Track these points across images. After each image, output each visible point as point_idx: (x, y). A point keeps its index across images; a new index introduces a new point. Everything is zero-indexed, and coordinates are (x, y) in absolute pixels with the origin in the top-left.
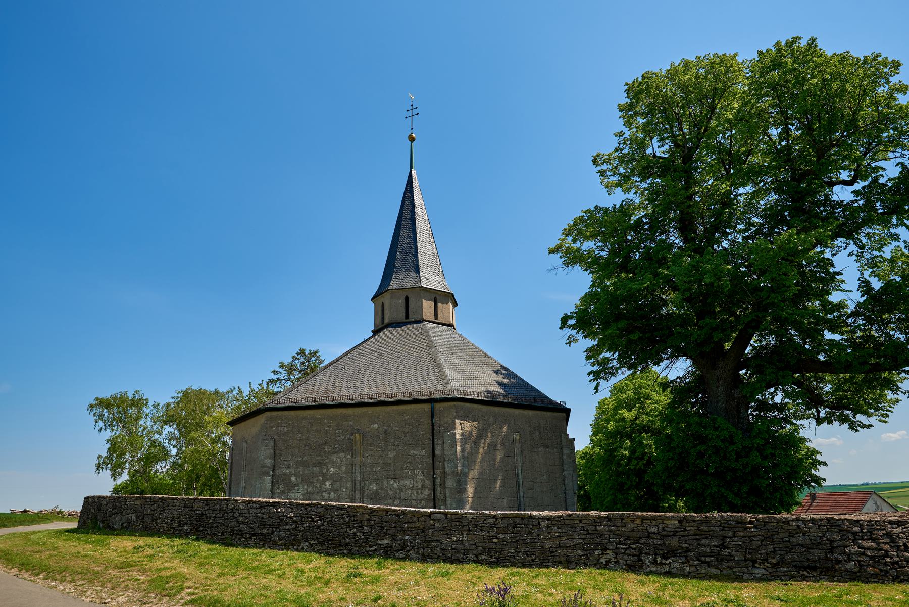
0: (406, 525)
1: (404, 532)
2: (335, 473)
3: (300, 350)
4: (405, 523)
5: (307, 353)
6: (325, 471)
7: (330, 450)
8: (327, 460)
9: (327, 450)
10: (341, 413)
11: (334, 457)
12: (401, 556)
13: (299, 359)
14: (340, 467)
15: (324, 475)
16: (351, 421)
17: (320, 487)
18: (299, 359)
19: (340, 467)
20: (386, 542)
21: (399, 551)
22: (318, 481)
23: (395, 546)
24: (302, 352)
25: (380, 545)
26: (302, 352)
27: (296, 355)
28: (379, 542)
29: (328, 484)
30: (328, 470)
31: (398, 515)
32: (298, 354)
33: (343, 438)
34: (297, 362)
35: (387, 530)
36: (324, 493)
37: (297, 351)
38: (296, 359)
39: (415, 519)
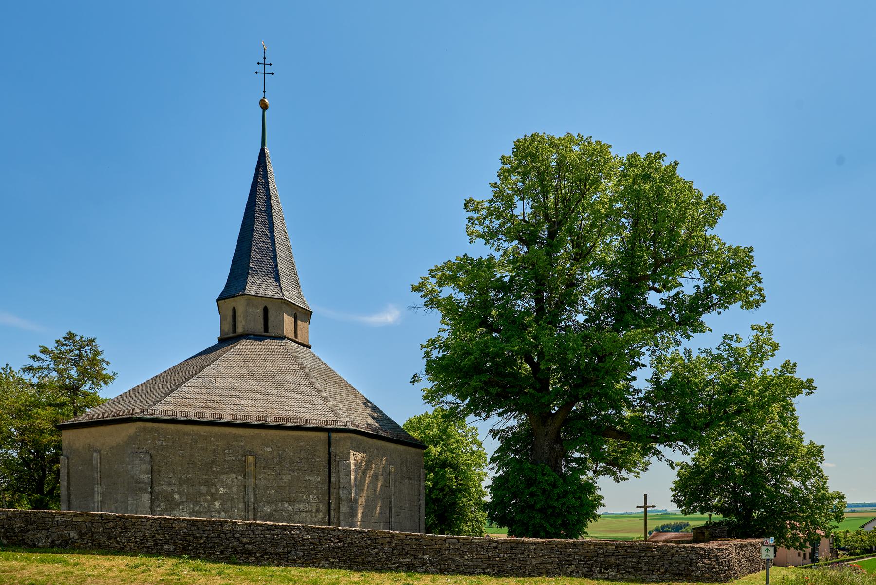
0: (425, 547)
1: (424, 552)
2: (225, 494)
3: (69, 334)
4: (424, 545)
5: (78, 338)
6: (213, 490)
7: (218, 469)
8: (216, 480)
9: (215, 469)
10: (230, 433)
11: (224, 477)
12: (422, 570)
13: (67, 345)
14: (230, 488)
15: (212, 495)
16: (242, 442)
17: (209, 506)
18: (67, 345)
19: (230, 488)
20: (408, 560)
21: (420, 567)
22: (206, 500)
23: (416, 563)
24: (70, 336)
25: (402, 562)
26: (70, 336)
27: (63, 340)
28: (401, 560)
29: (217, 504)
30: (217, 490)
31: (416, 539)
32: (66, 339)
33: (234, 458)
34: (63, 349)
35: (408, 551)
36: (213, 513)
37: (65, 335)
38: (63, 345)
39: (433, 543)
